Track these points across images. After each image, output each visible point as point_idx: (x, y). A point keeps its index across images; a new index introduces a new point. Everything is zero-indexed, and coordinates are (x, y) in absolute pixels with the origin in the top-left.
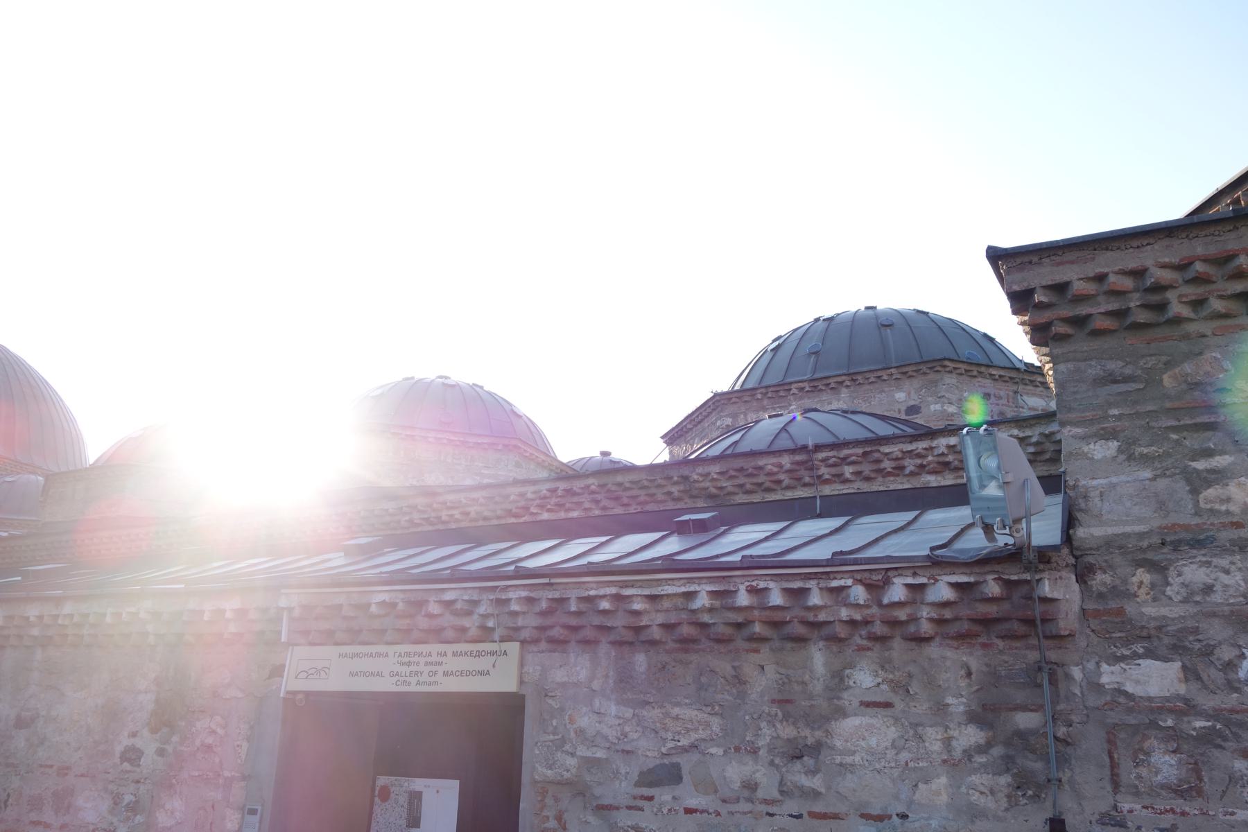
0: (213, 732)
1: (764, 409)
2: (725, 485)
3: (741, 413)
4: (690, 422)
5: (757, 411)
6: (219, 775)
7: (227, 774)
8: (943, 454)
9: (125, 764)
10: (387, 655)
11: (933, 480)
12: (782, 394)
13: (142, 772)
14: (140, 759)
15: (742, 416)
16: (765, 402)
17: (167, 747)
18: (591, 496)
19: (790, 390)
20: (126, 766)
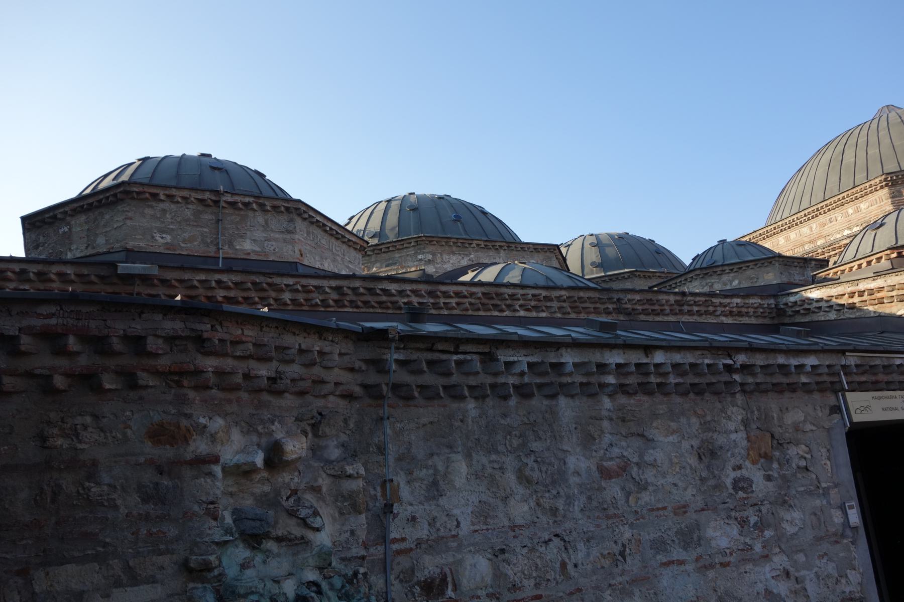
0: (802, 457)
1: (453, 253)
2: (638, 308)
3: (438, 253)
4: (373, 251)
5: (449, 254)
6: (818, 487)
7: (824, 485)
8: (733, 307)
9: (740, 492)
10: (896, 398)
11: (725, 320)
12: (467, 245)
13: (758, 496)
14: (752, 487)
15: (439, 255)
16: (454, 249)
17: (771, 473)
18: (560, 303)
19: (471, 244)
20: (741, 494)
